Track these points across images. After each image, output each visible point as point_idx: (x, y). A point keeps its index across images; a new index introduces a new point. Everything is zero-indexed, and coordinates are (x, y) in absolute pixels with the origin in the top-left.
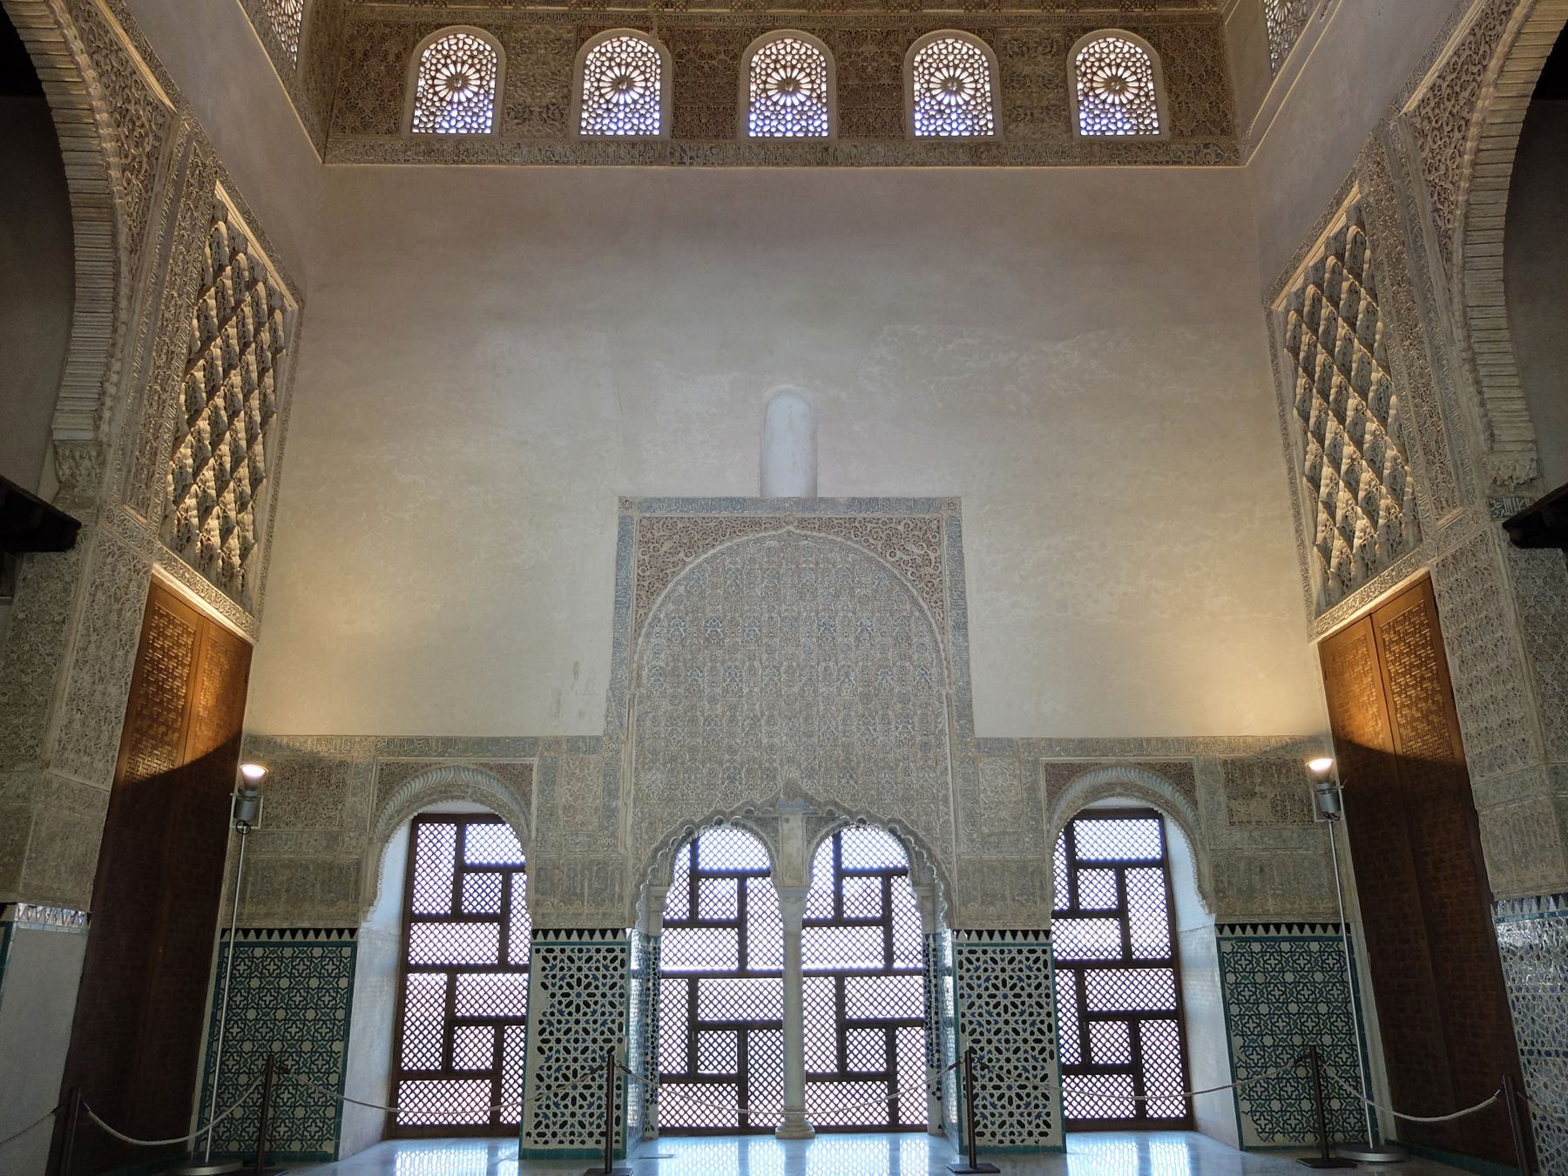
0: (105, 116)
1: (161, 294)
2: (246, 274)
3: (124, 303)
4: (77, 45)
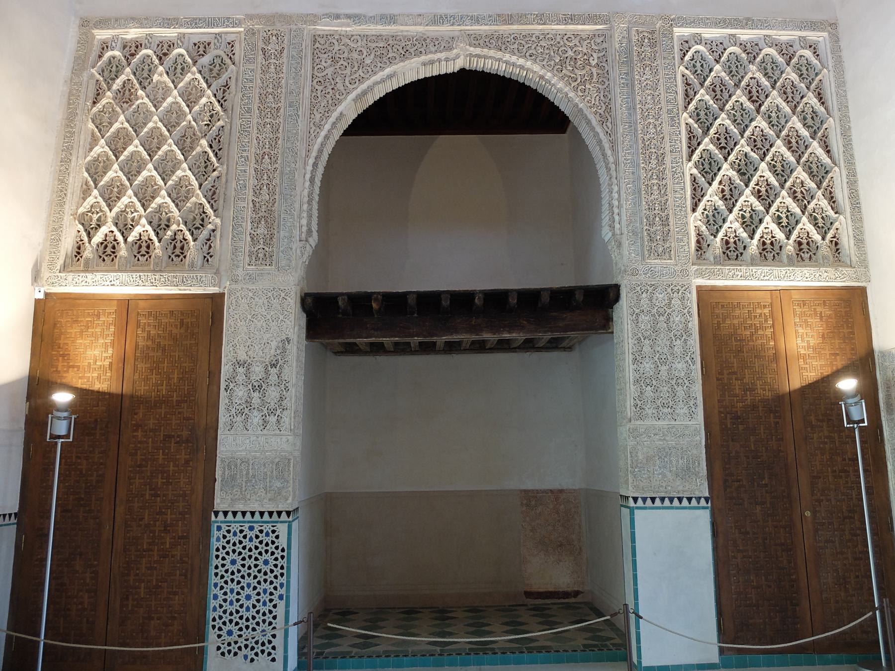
0: (549, 74)
1: (636, 130)
2: (744, 55)
3: (609, 152)
4: (514, 59)
